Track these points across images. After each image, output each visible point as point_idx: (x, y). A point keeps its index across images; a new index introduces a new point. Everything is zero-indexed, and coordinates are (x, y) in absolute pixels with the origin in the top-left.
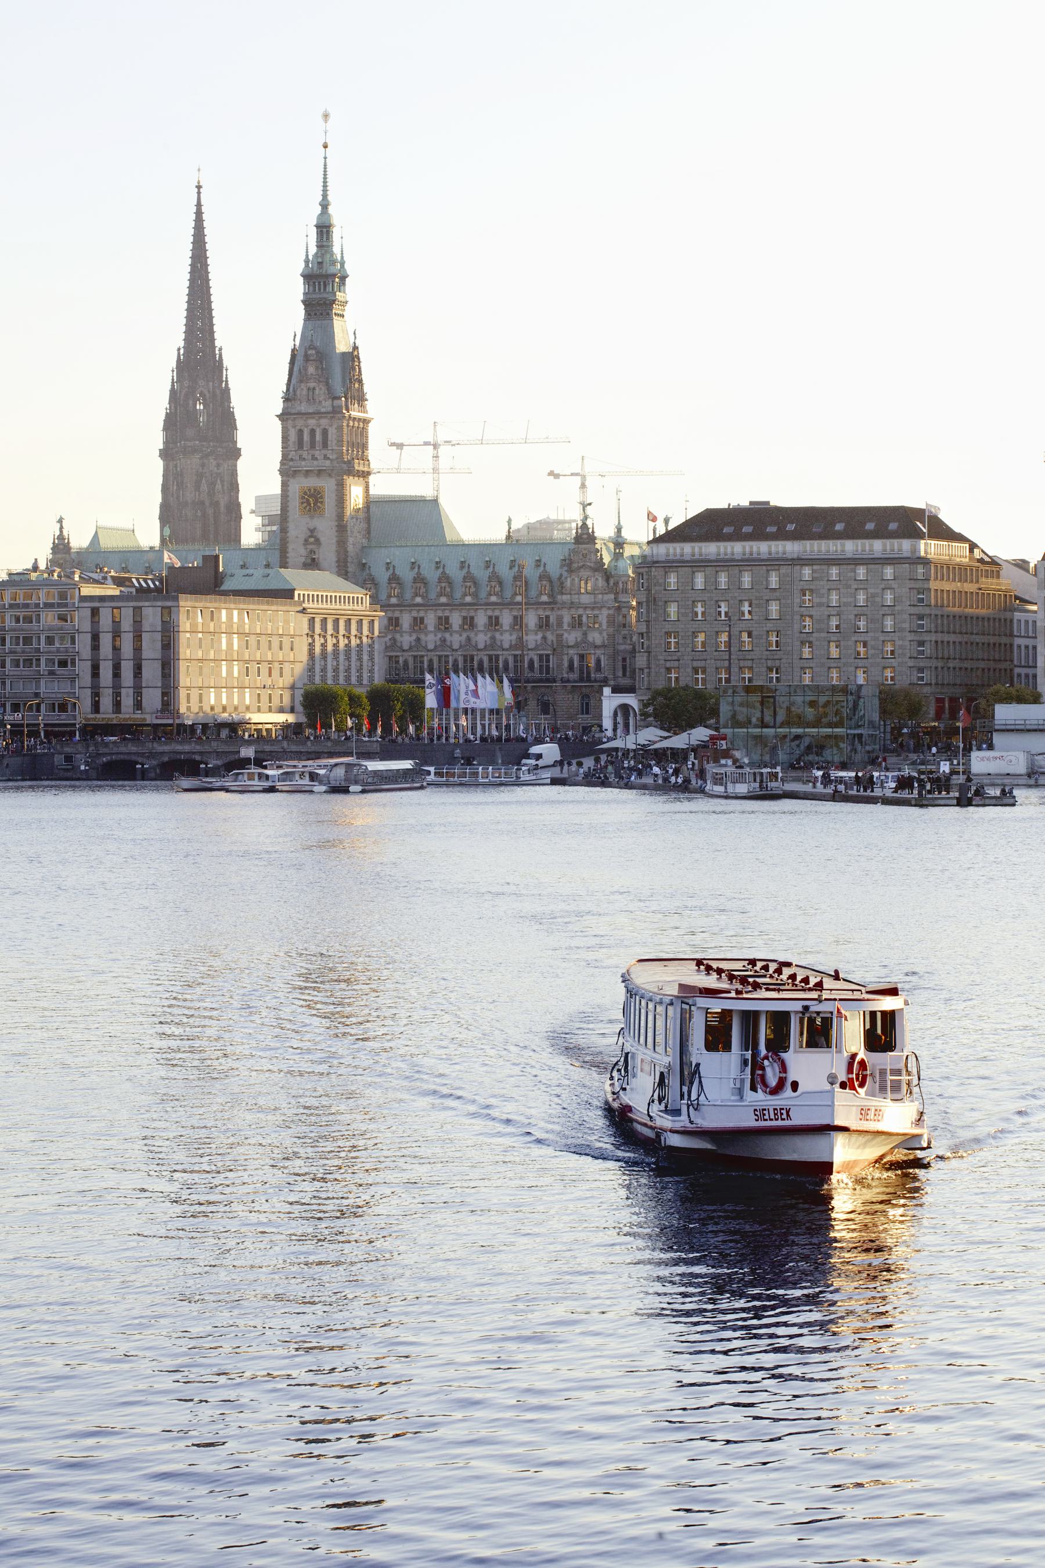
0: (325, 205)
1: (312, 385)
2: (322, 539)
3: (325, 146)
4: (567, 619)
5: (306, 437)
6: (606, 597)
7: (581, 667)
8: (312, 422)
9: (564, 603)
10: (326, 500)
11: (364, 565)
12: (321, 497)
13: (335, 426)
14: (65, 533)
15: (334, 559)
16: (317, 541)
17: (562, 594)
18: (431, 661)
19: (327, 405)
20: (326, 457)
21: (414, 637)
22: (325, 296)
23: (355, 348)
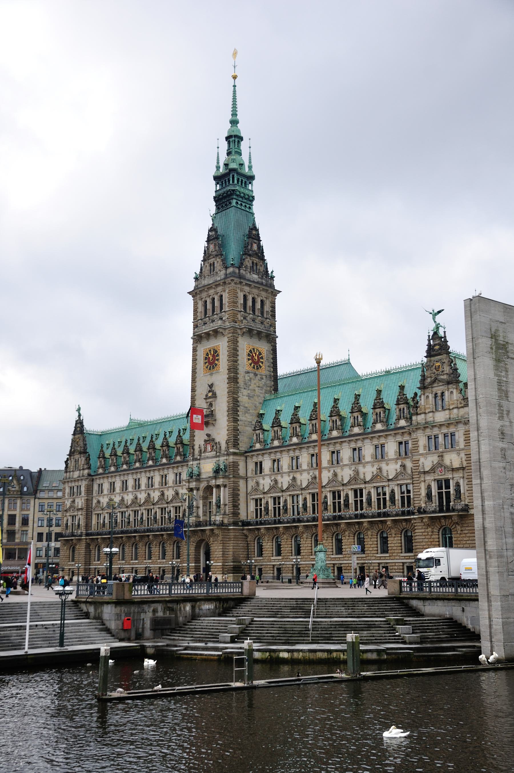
0: (234, 122)
1: (211, 261)
3: (235, 77)
4: (422, 441)
5: (209, 306)
6: (462, 411)
7: (440, 494)
8: (212, 292)
9: (418, 424)
11: (261, 416)
12: (218, 355)
13: (227, 291)
14: (81, 418)
15: (226, 409)
16: (214, 396)
17: (417, 414)
18: (305, 499)
19: (222, 274)
20: (221, 319)
21: (291, 477)
23: (254, 228)
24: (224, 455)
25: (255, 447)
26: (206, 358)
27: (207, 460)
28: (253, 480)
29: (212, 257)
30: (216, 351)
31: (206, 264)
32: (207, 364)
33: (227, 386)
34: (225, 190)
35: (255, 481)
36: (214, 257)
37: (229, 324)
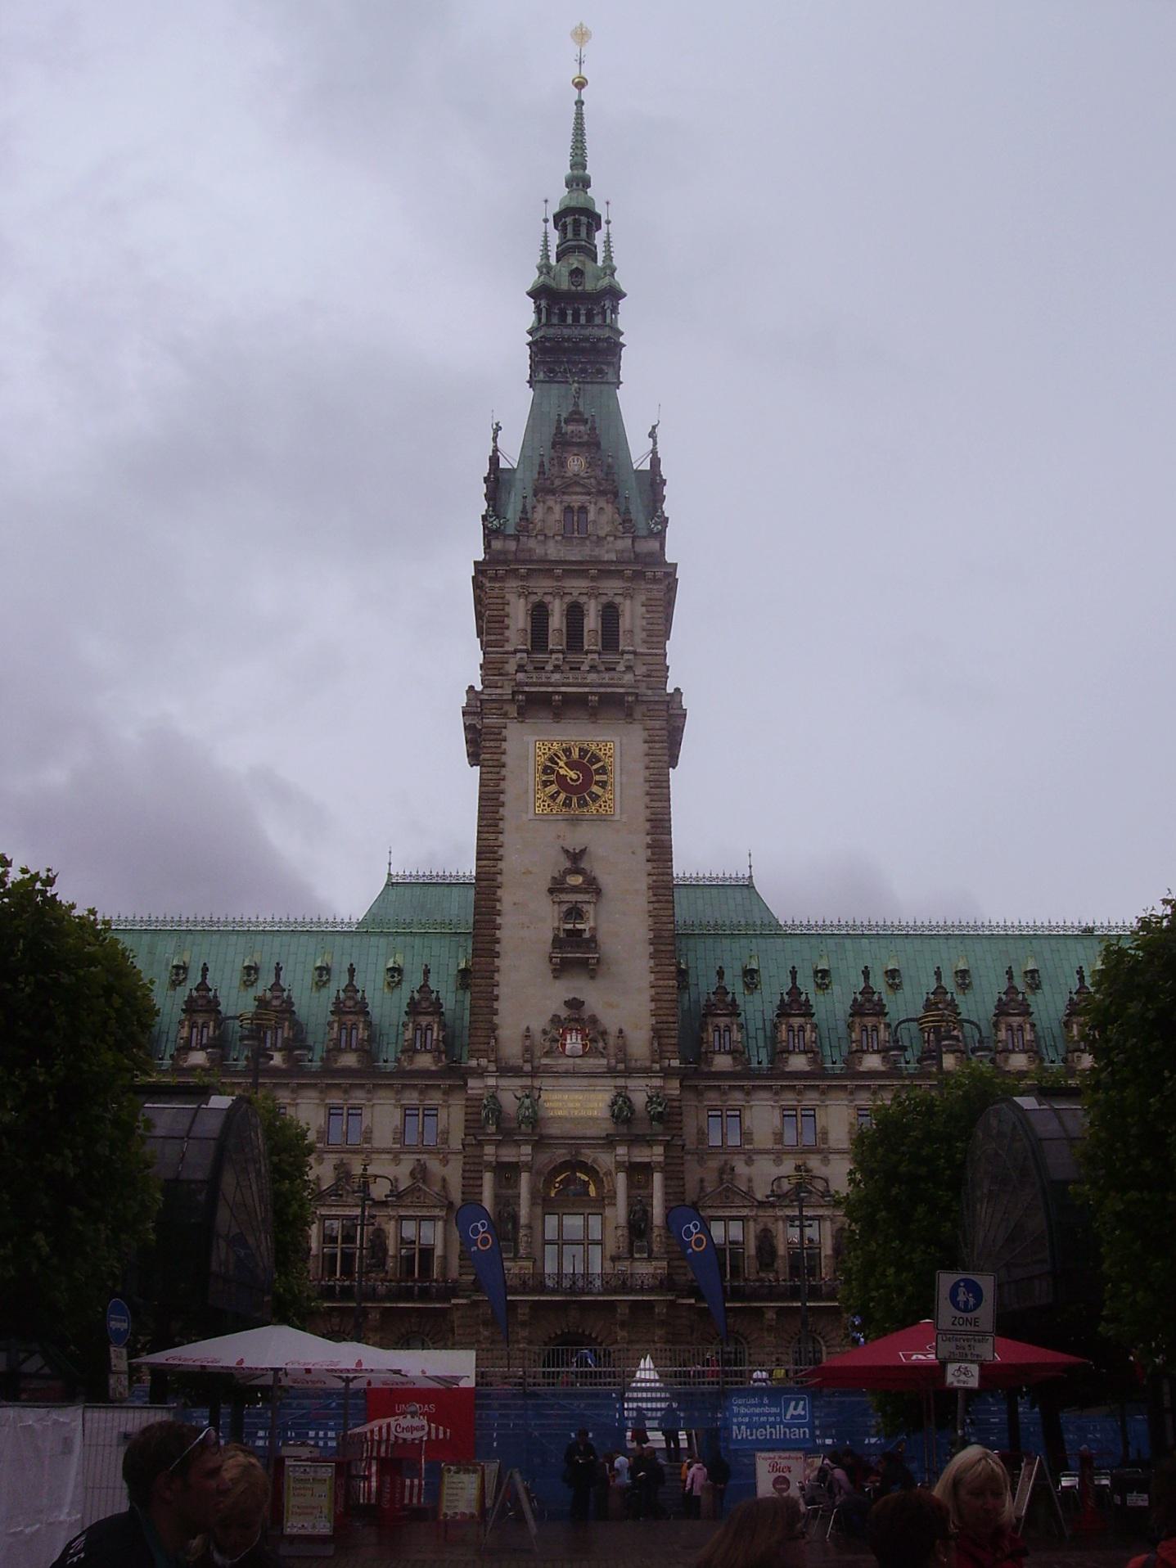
2: (605, 879)
3: (580, 84)
5: (556, 621)
8: (577, 586)
10: (616, 777)
16: (592, 887)
22: (597, 332)
24: (647, 1072)
25: (710, 1063)
26: (546, 770)
27: (562, 1081)
28: (701, 1161)
29: (578, 489)
30: (595, 759)
31: (550, 503)
32: (554, 788)
33: (649, 866)
34: (587, 332)
35: (714, 1164)
36: (589, 494)
37: (650, 692)
